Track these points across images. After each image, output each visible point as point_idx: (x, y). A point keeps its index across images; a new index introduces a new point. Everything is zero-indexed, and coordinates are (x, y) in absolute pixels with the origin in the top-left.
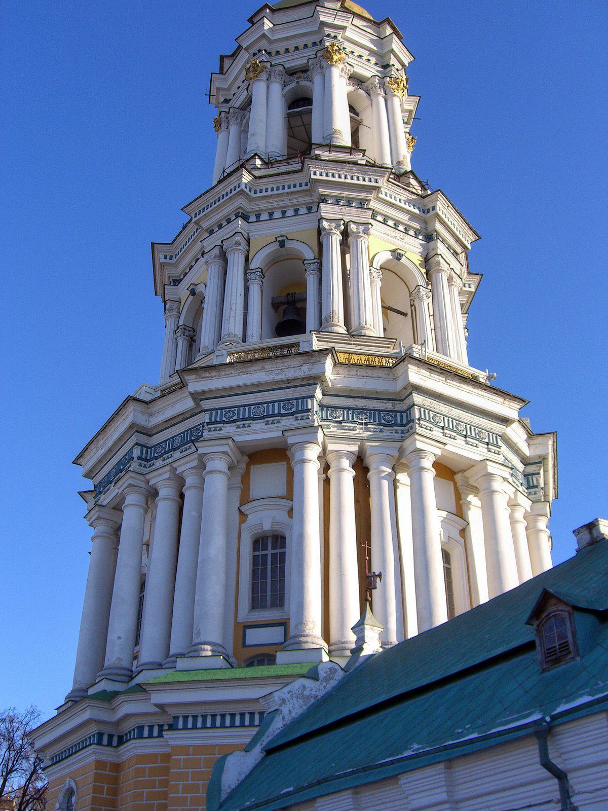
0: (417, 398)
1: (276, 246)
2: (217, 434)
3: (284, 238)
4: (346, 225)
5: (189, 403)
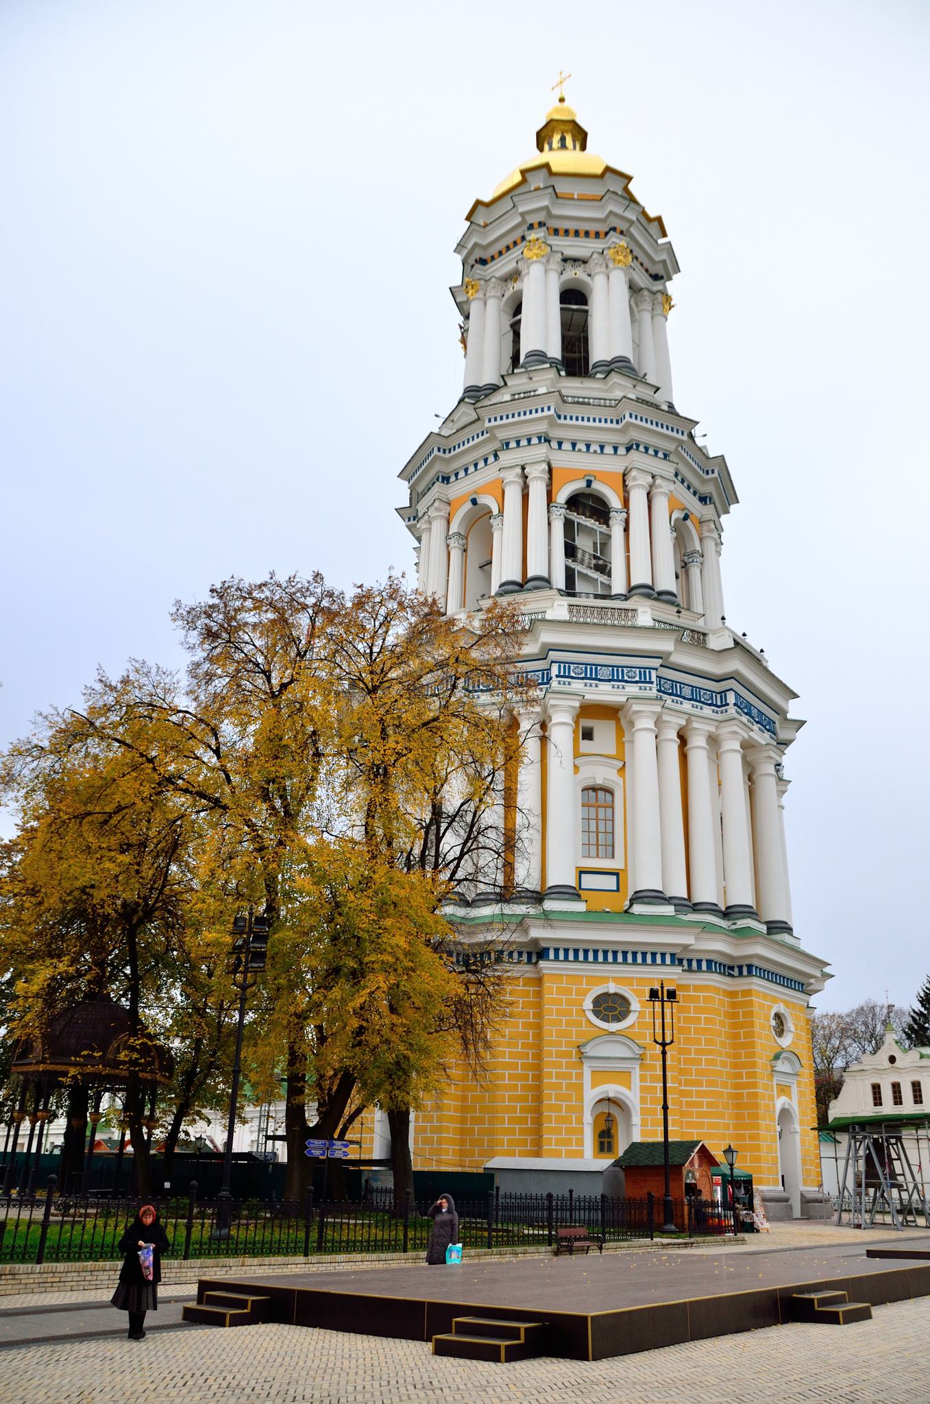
0: (553, 655)
1: (469, 505)
4: (523, 468)
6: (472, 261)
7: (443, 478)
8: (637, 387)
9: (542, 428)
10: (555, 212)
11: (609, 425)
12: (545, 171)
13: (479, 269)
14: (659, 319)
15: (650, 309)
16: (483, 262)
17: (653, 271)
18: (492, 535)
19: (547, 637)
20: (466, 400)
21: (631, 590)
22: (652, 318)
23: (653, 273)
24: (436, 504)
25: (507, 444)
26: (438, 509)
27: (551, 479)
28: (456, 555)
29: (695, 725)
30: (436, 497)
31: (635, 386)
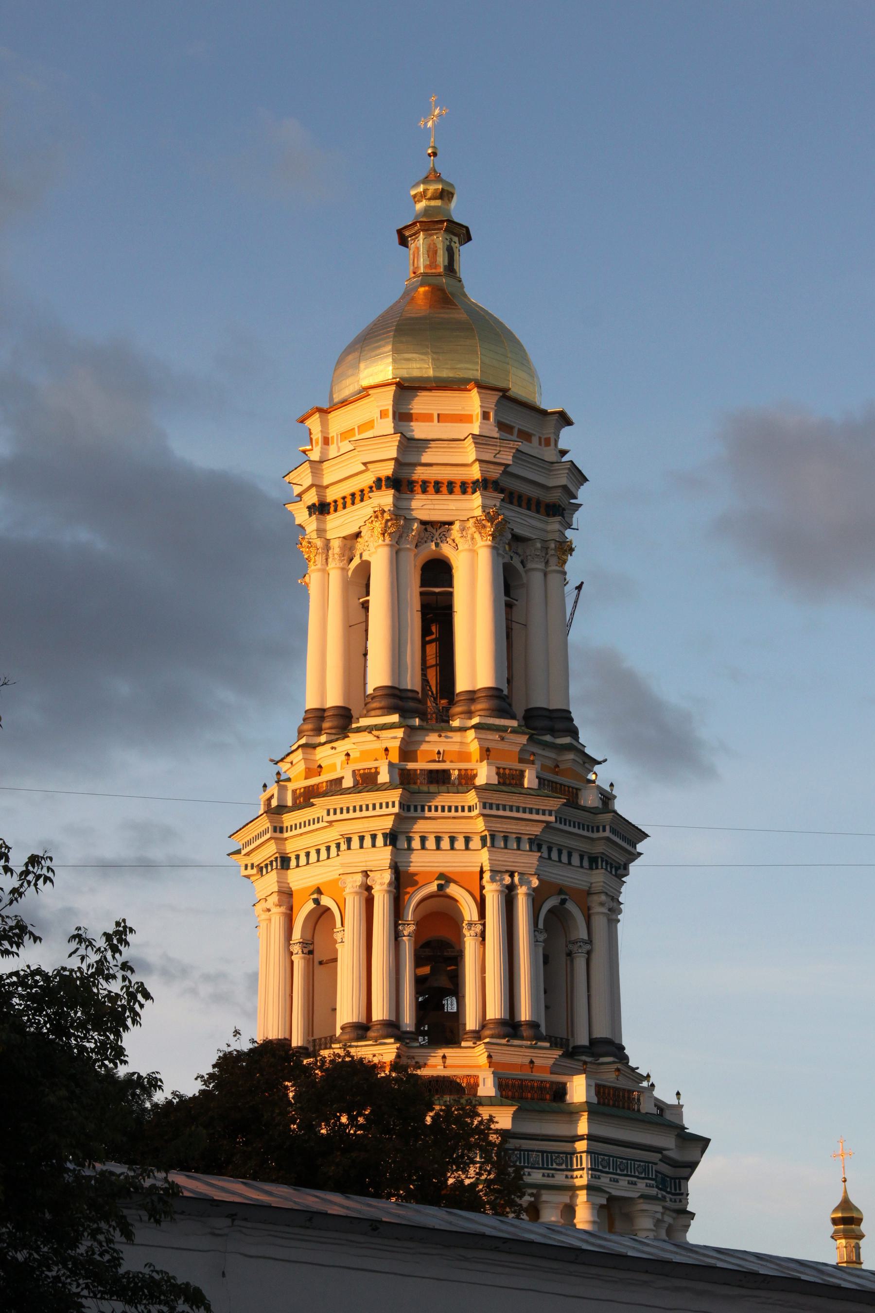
1: (311, 905)
3: (315, 896)
14: (554, 579)
15: (541, 566)
22: (545, 574)
25: (349, 840)
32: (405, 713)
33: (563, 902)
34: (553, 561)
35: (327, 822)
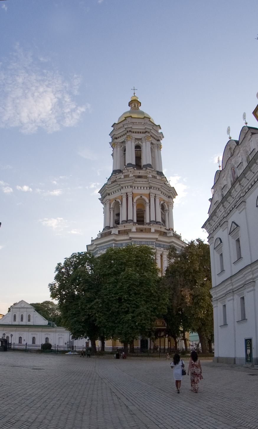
0: (133, 240)
1: (114, 201)
2: (100, 252)
4: (127, 193)
5: (95, 246)
6: (113, 138)
7: (108, 194)
8: (153, 172)
9: (131, 184)
10: (133, 128)
11: (145, 182)
12: (130, 117)
13: (116, 140)
16: (116, 138)
17: (157, 139)
18: (120, 208)
19: (131, 235)
20: (113, 174)
21: (150, 221)
22: (158, 150)
23: (158, 139)
24: (107, 201)
25: (123, 188)
26: (107, 202)
27: (133, 196)
28: (112, 212)
29: (164, 253)
30: (107, 199)
31: (152, 172)
32: (134, 168)
33: (164, 202)
34: (159, 148)
35: (119, 184)
